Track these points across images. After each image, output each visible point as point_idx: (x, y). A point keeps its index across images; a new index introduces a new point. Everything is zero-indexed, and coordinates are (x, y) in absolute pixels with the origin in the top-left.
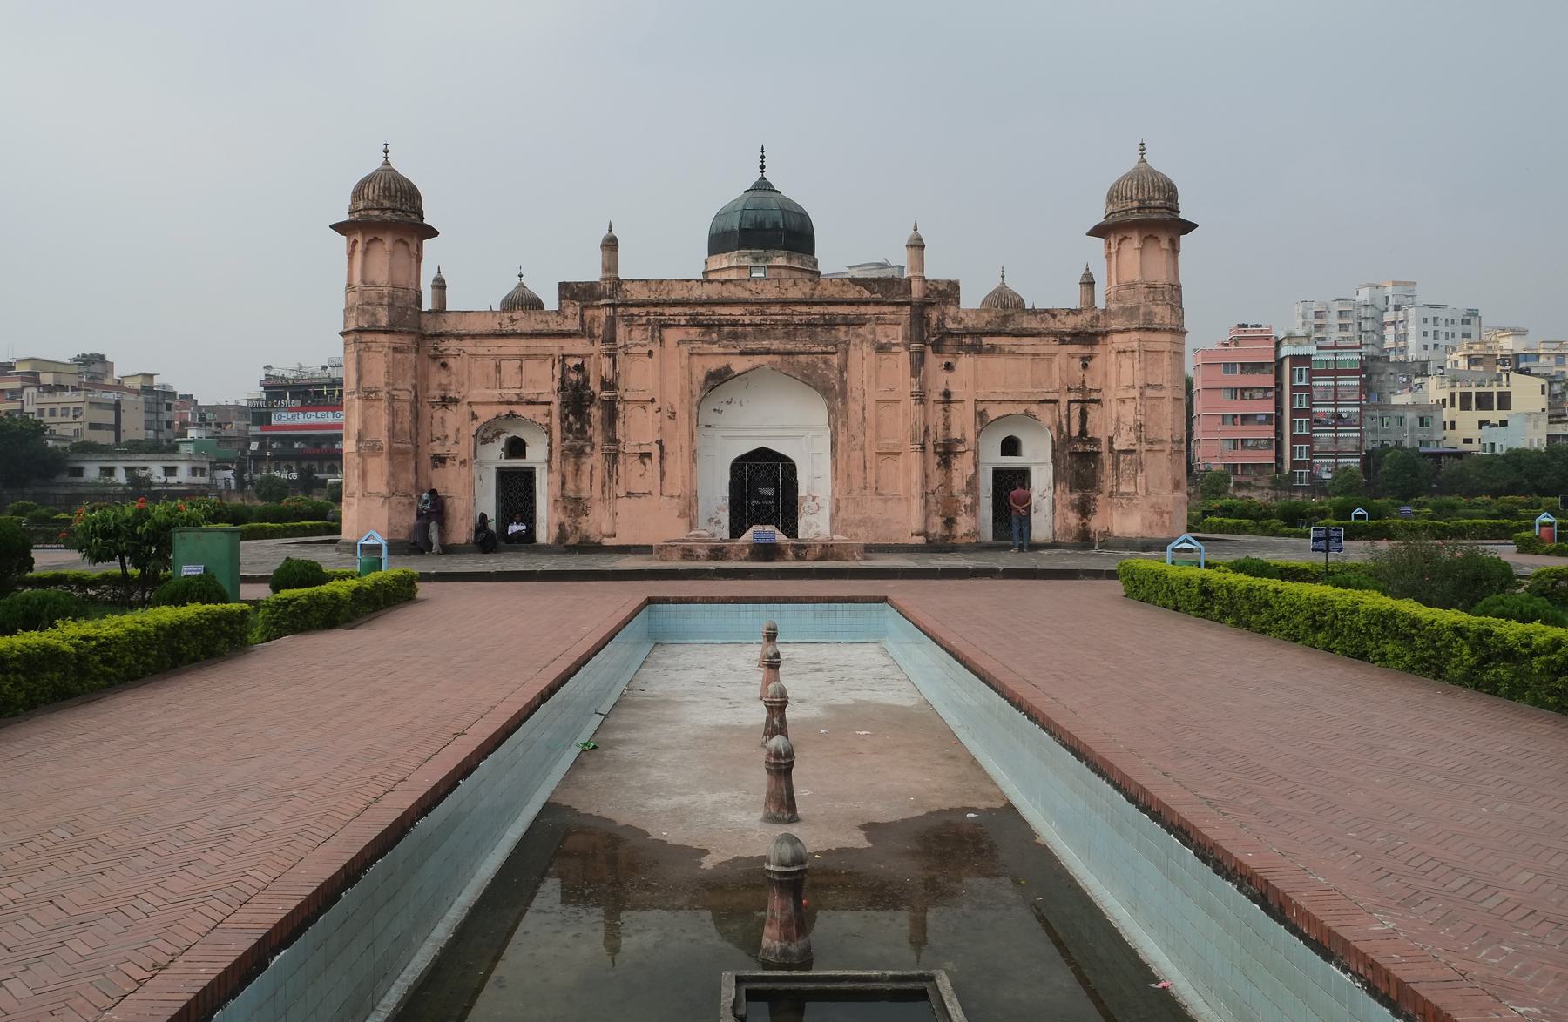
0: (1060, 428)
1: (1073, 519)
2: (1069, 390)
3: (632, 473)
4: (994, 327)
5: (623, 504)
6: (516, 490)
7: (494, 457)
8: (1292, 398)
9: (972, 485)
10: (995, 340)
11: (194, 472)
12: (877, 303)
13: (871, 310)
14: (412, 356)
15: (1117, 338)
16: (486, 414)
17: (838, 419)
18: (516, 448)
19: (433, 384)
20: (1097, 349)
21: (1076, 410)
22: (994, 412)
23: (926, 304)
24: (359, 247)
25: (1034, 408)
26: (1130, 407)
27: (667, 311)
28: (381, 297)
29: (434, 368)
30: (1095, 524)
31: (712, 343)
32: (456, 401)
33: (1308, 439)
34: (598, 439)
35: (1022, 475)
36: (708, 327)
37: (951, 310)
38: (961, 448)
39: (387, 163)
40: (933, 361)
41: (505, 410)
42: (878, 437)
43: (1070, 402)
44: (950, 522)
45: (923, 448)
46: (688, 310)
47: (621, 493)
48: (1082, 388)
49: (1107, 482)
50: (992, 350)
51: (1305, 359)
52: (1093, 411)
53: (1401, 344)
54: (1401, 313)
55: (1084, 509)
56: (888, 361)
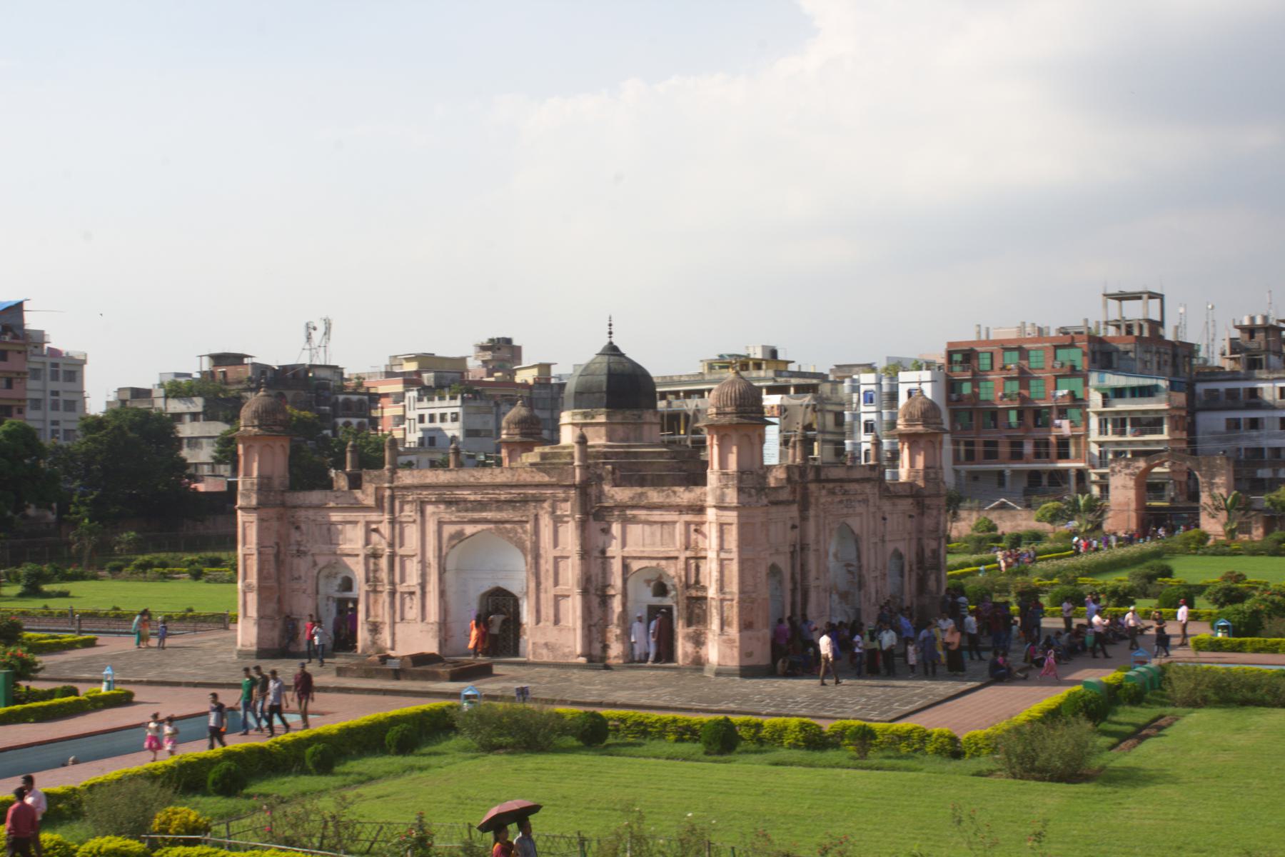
2: (687, 548)
4: (634, 502)
14: (275, 525)
16: (322, 561)
19: (293, 541)
22: (636, 565)
25: (663, 563)
29: (293, 531)
31: (451, 513)
32: (305, 553)
35: (670, 609)
36: (449, 503)
40: (595, 526)
42: (556, 583)
43: (687, 559)
44: (605, 647)
47: (398, 619)
48: (696, 549)
50: (634, 520)
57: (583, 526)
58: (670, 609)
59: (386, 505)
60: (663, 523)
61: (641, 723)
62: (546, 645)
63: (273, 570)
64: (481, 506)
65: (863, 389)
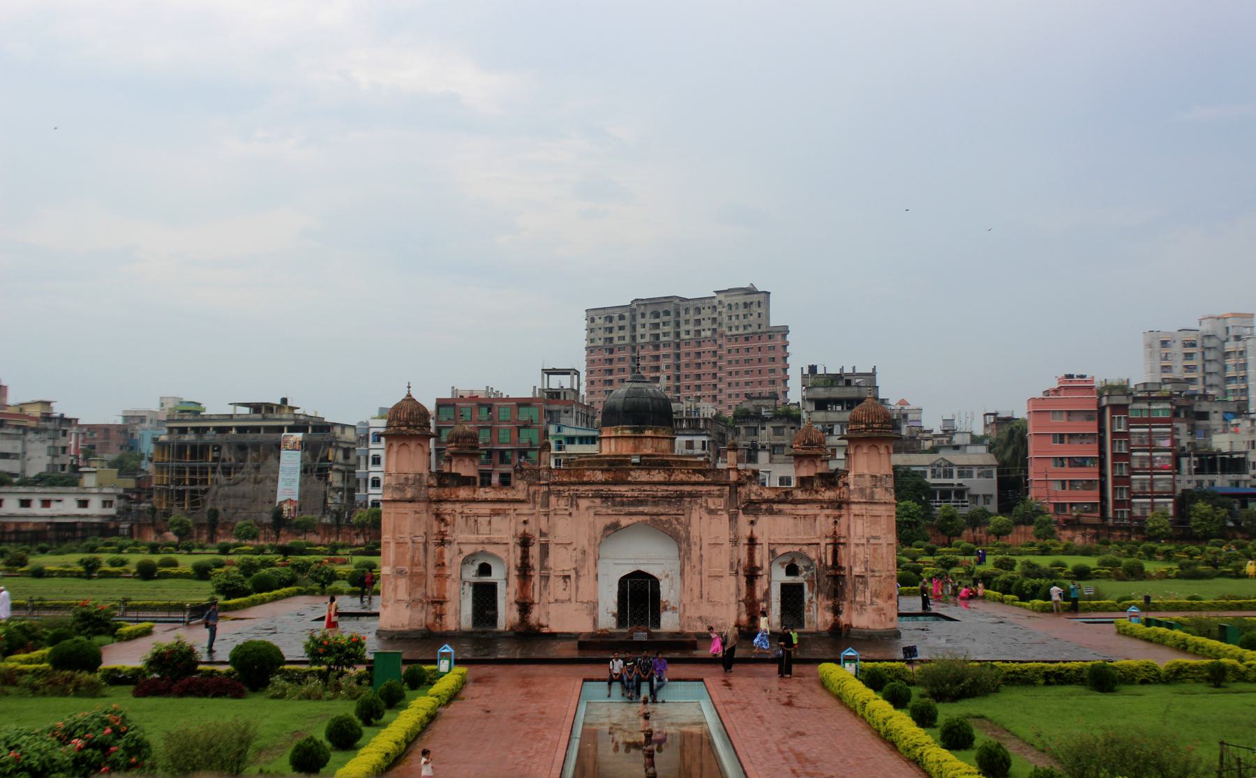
0: (820, 561)
1: (829, 617)
3: (556, 586)
5: (553, 608)
6: (485, 596)
7: (471, 574)
8: (1113, 443)
9: (767, 594)
10: (781, 506)
11: (106, 504)
12: (708, 484)
13: (705, 489)
15: (853, 506)
16: (468, 550)
17: (684, 556)
18: (485, 569)
20: (844, 512)
21: (830, 548)
22: (780, 551)
23: (739, 484)
24: (395, 448)
25: (805, 548)
26: (861, 548)
27: (582, 488)
28: (407, 479)
30: (843, 619)
31: (608, 507)
32: (450, 543)
33: (1127, 481)
34: (537, 567)
35: (801, 586)
36: (605, 498)
37: (755, 488)
38: (760, 573)
39: (409, 395)
40: (743, 520)
41: (480, 548)
45: (737, 573)
46: (594, 488)
49: (849, 595)
50: (780, 512)
51: (1123, 408)
52: (842, 552)
53: (1242, 373)
54: (1240, 344)
55: (836, 611)
56: (715, 520)
57: (733, 518)
58: (801, 586)
59: (539, 500)
60: (805, 516)
61: (1014, 672)
62: (700, 618)
63: (422, 558)
64: (638, 502)
65: (372, 431)
